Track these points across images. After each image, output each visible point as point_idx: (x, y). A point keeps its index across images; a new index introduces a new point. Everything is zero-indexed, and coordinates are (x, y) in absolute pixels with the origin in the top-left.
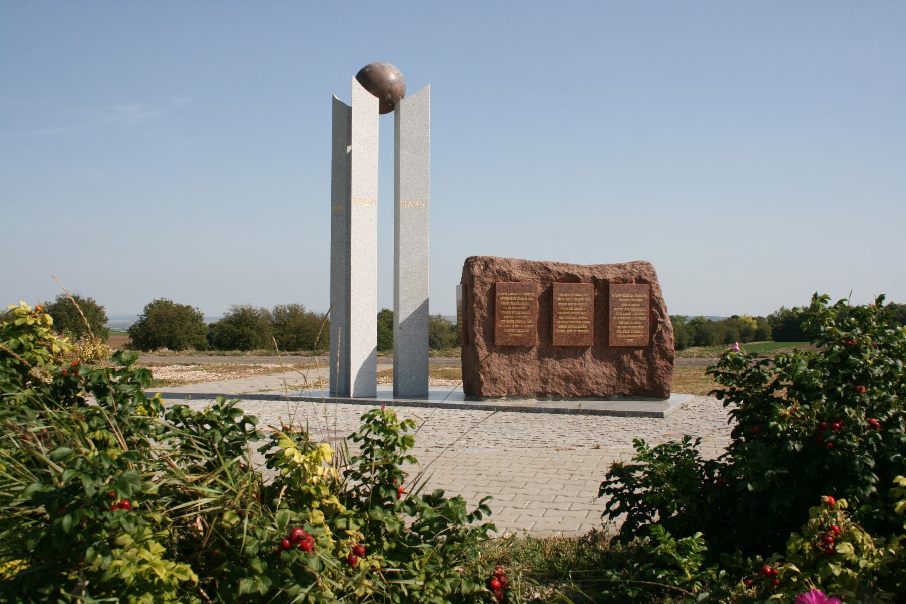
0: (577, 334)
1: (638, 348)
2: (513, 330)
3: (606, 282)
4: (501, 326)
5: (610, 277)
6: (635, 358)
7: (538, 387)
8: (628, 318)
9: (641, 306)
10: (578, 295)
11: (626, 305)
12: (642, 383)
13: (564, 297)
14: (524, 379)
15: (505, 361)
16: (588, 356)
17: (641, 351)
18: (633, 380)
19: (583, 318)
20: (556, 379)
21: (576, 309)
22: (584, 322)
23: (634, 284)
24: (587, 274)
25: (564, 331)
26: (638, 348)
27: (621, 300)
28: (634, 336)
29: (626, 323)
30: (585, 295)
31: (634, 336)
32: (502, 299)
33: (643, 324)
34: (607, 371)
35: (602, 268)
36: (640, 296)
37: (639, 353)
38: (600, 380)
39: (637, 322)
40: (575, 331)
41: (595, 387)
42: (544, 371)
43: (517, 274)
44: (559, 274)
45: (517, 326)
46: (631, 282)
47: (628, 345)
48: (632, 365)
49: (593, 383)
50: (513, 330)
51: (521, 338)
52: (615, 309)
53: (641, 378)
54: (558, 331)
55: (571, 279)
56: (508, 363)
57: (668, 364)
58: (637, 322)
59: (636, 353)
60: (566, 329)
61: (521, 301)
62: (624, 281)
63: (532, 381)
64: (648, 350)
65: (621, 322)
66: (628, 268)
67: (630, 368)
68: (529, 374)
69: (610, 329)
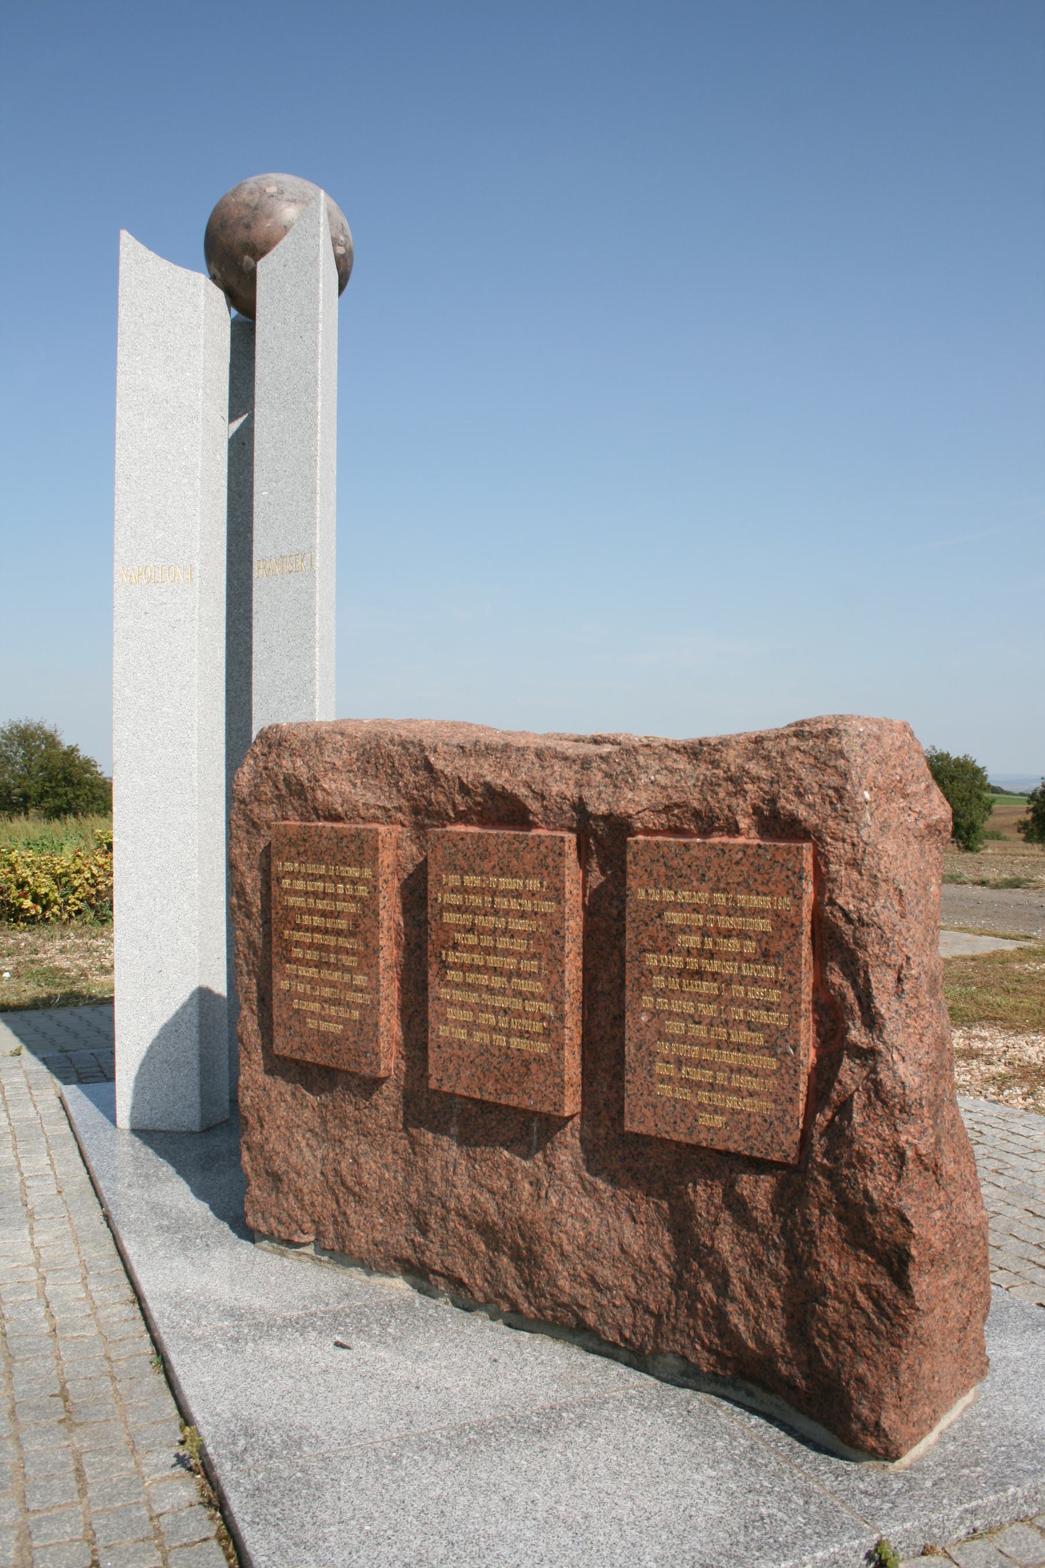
0: (506, 1054)
1: (758, 1165)
2: (315, 1007)
3: (619, 827)
4: (284, 985)
5: (635, 801)
6: (738, 1208)
7: (400, 1236)
8: (709, 1011)
9: (766, 956)
10: (506, 883)
11: (693, 941)
12: (759, 1337)
13: (464, 890)
14: (359, 1199)
15: (307, 1113)
16: (567, 1153)
17: (766, 1183)
18: (721, 1316)
19: (525, 986)
20: (454, 1221)
21: (504, 943)
22: (533, 1006)
23: (749, 838)
24: (561, 785)
25: (462, 1035)
26: (758, 1165)
27: (675, 918)
28: (732, 1102)
29: (700, 1031)
30: (533, 884)
31: (732, 1102)
32: (286, 883)
33: (770, 1048)
34: (630, 1234)
35: (621, 758)
36: (757, 901)
37: (758, 1191)
38: (605, 1273)
39: (743, 1036)
40: (501, 1040)
41: (584, 1294)
42: (418, 1180)
43: (338, 788)
44: (464, 789)
45: (327, 992)
46: (734, 830)
47: (703, 1138)
48: (725, 1244)
49: (574, 1277)
50: (315, 1007)
51: (338, 1039)
52: (652, 960)
53: (758, 1319)
54: (443, 1031)
55: (503, 810)
56: (316, 1123)
57: (883, 1283)
58: (743, 1036)
59: (747, 1185)
60: (471, 1027)
61: (335, 897)
62: (707, 823)
63: (383, 1211)
64: (792, 1178)
65: (675, 1027)
66: (732, 758)
67: (712, 1250)
68: (372, 1183)
69: (630, 1049)
